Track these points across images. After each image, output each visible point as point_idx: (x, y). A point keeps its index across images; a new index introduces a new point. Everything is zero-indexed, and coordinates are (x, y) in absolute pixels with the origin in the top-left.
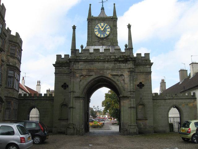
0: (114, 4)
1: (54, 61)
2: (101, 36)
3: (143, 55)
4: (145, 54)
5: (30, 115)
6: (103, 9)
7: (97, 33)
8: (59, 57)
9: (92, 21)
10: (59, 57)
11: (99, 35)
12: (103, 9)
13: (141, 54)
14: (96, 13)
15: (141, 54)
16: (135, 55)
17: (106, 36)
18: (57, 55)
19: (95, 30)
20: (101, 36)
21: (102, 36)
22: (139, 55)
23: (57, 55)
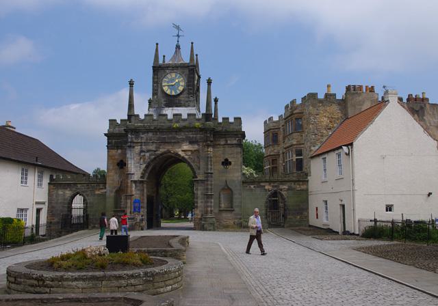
0: (192, 43)
1: (106, 128)
2: (171, 92)
3: (231, 120)
4: (235, 119)
5: (73, 205)
6: (178, 47)
7: (165, 89)
8: (112, 122)
9: (159, 70)
10: (112, 122)
11: (168, 92)
12: (178, 47)
13: (228, 119)
14: (167, 56)
15: (228, 119)
16: (220, 120)
17: (178, 92)
18: (110, 120)
19: (163, 84)
20: (171, 92)
21: (173, 93)
22: (226, 119)
23: (110, 120)
